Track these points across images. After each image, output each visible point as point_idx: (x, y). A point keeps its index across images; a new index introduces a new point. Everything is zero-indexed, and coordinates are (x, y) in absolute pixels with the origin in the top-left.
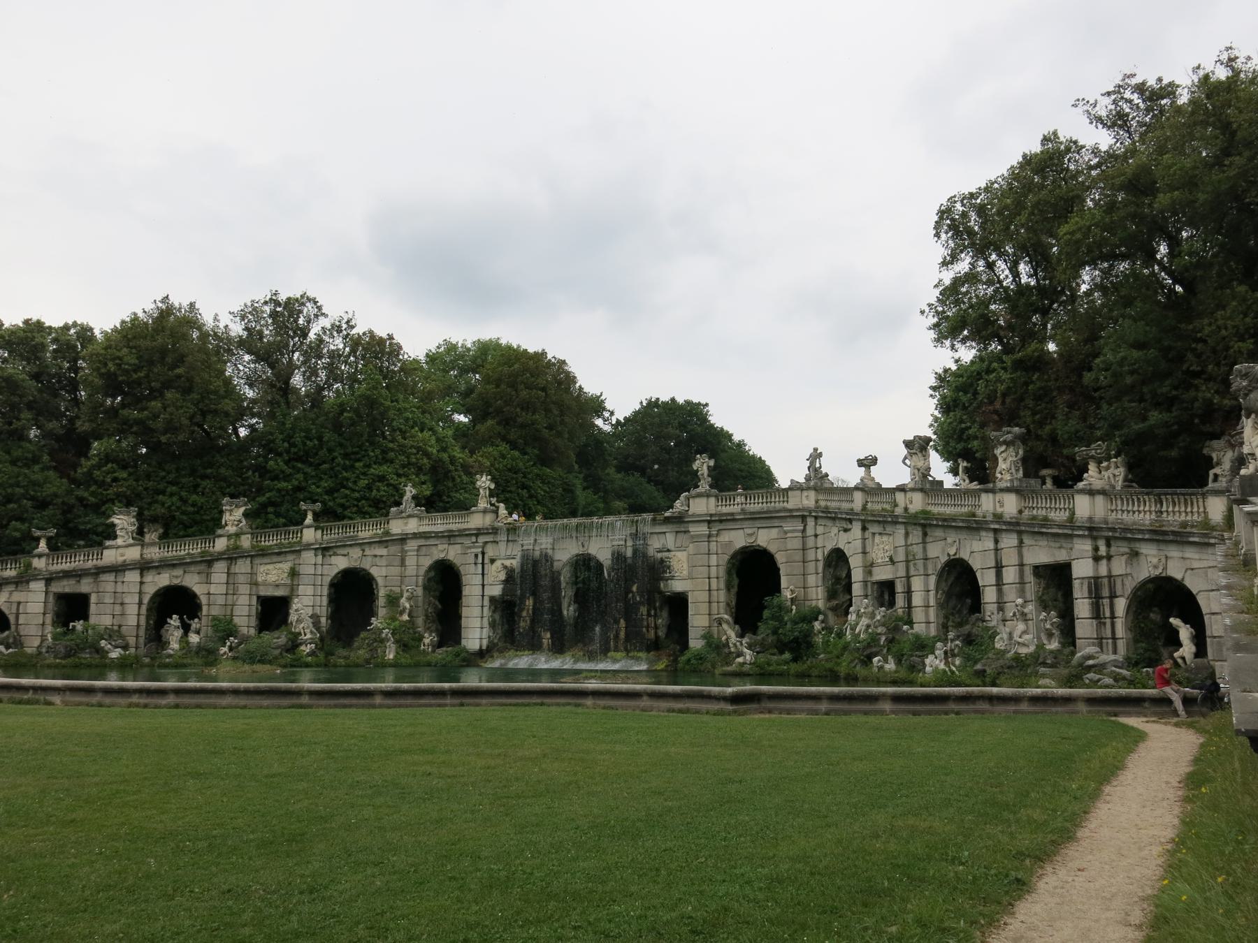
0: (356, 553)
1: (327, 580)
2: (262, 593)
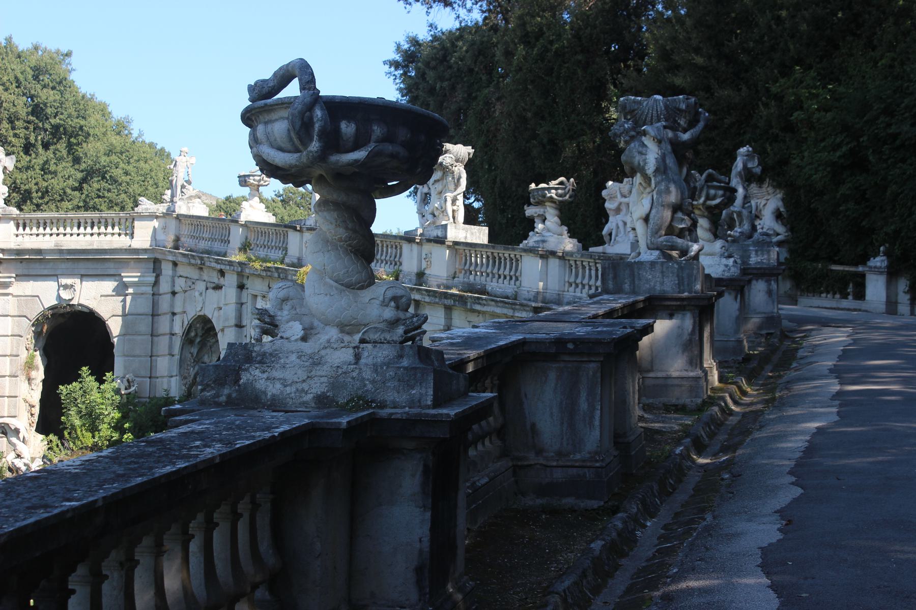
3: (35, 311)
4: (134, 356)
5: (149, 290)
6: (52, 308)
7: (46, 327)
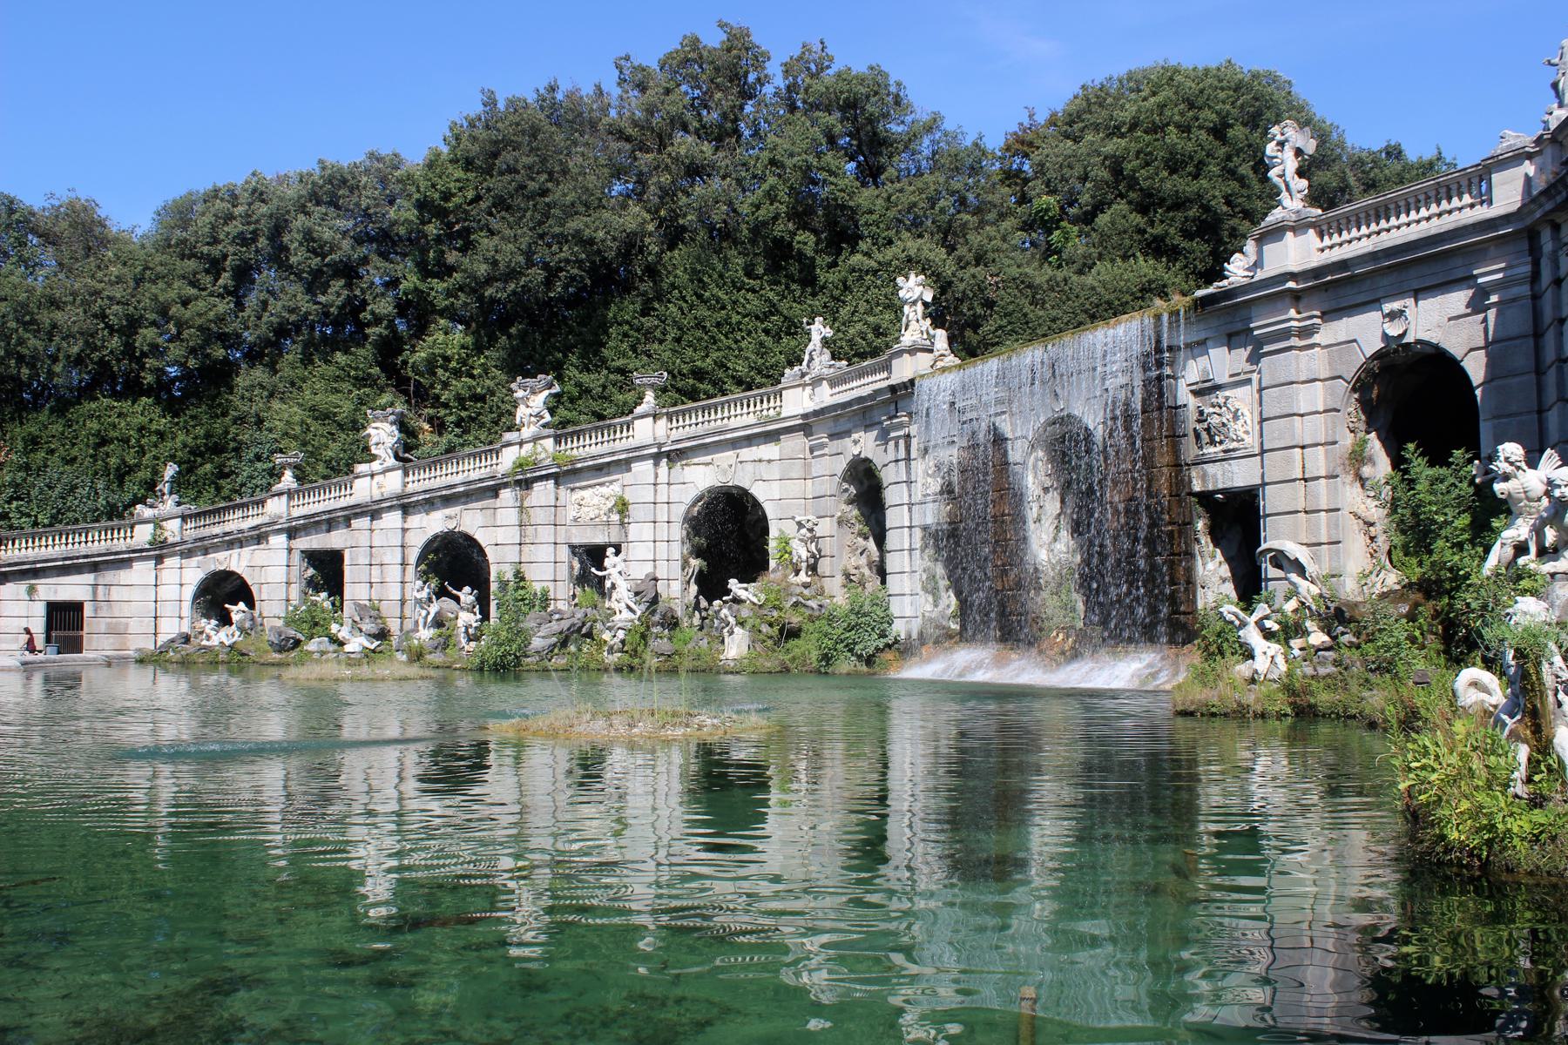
0: (727, 457)
1: (679, 512)
2: (576, 541)
3: (1351, 368)
4: (1509, 416)
5: (1525, 290)
6: (1378, 356)
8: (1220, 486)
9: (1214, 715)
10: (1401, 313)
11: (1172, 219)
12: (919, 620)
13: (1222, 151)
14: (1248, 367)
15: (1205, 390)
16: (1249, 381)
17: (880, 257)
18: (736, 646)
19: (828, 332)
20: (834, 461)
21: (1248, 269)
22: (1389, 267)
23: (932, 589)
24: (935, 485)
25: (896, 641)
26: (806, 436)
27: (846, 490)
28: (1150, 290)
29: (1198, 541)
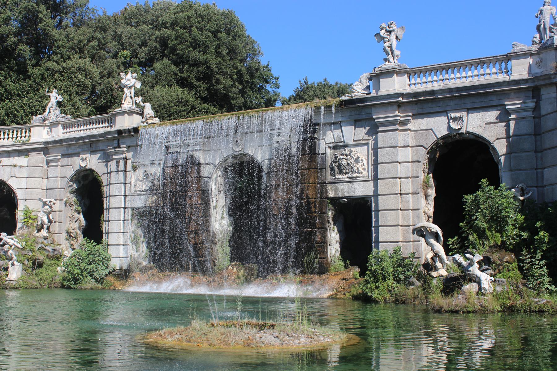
6: (444, 138)
7: (438, 154)
8: (347, 195)
9: (469, 312)
10: (460, 118)
11: (192, 71)
12: (129, 259)
13: (216, 43)
14: (366, 137)
15: (338, 146)
16: (367, 144)
17: (64, 65)
18: (15, 273)
19: (60, 98)
20: (65, 169)
21: (364, 90)
22: (456, 96)
23: (135, 241)
24: (145, 186)
25: (114, 271)
26: (45, 154)
27: (71, 186)
28: (181, 102)
29: (329, 222)
